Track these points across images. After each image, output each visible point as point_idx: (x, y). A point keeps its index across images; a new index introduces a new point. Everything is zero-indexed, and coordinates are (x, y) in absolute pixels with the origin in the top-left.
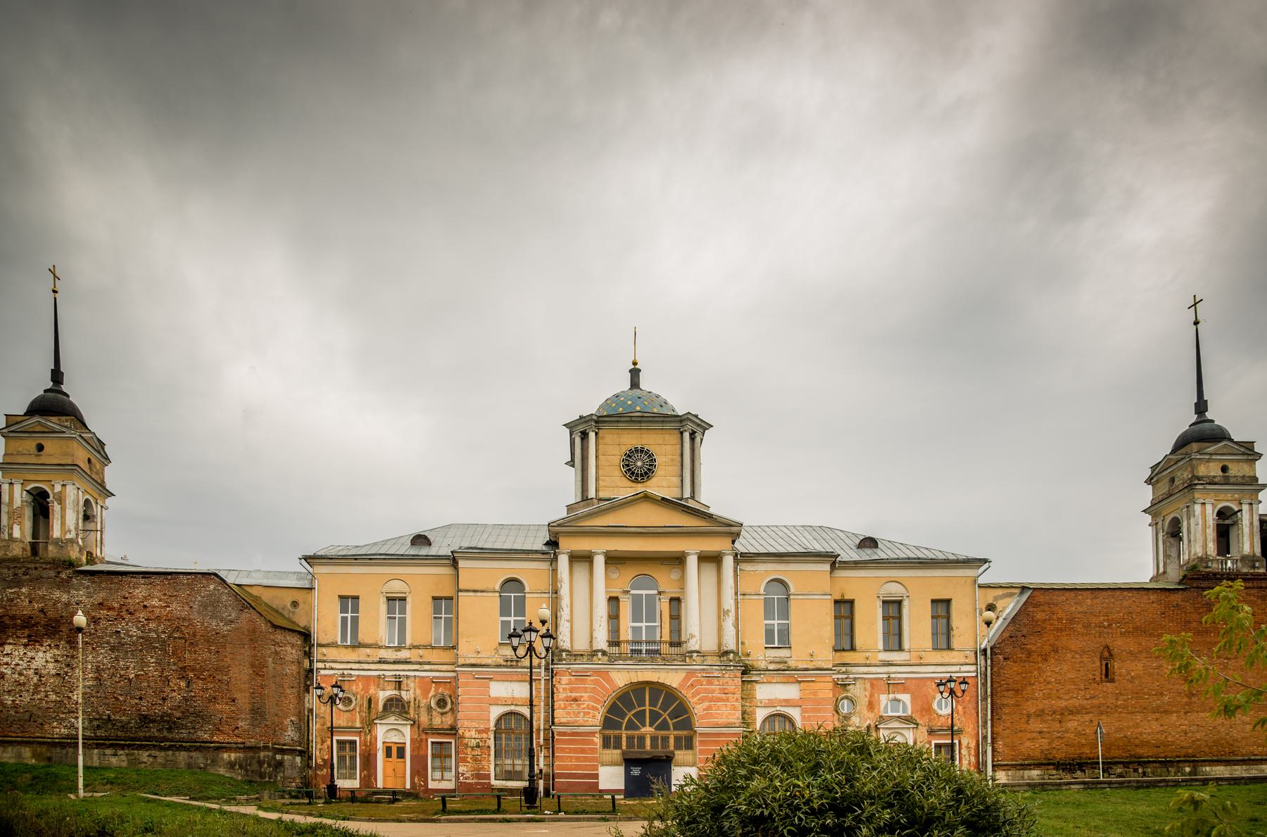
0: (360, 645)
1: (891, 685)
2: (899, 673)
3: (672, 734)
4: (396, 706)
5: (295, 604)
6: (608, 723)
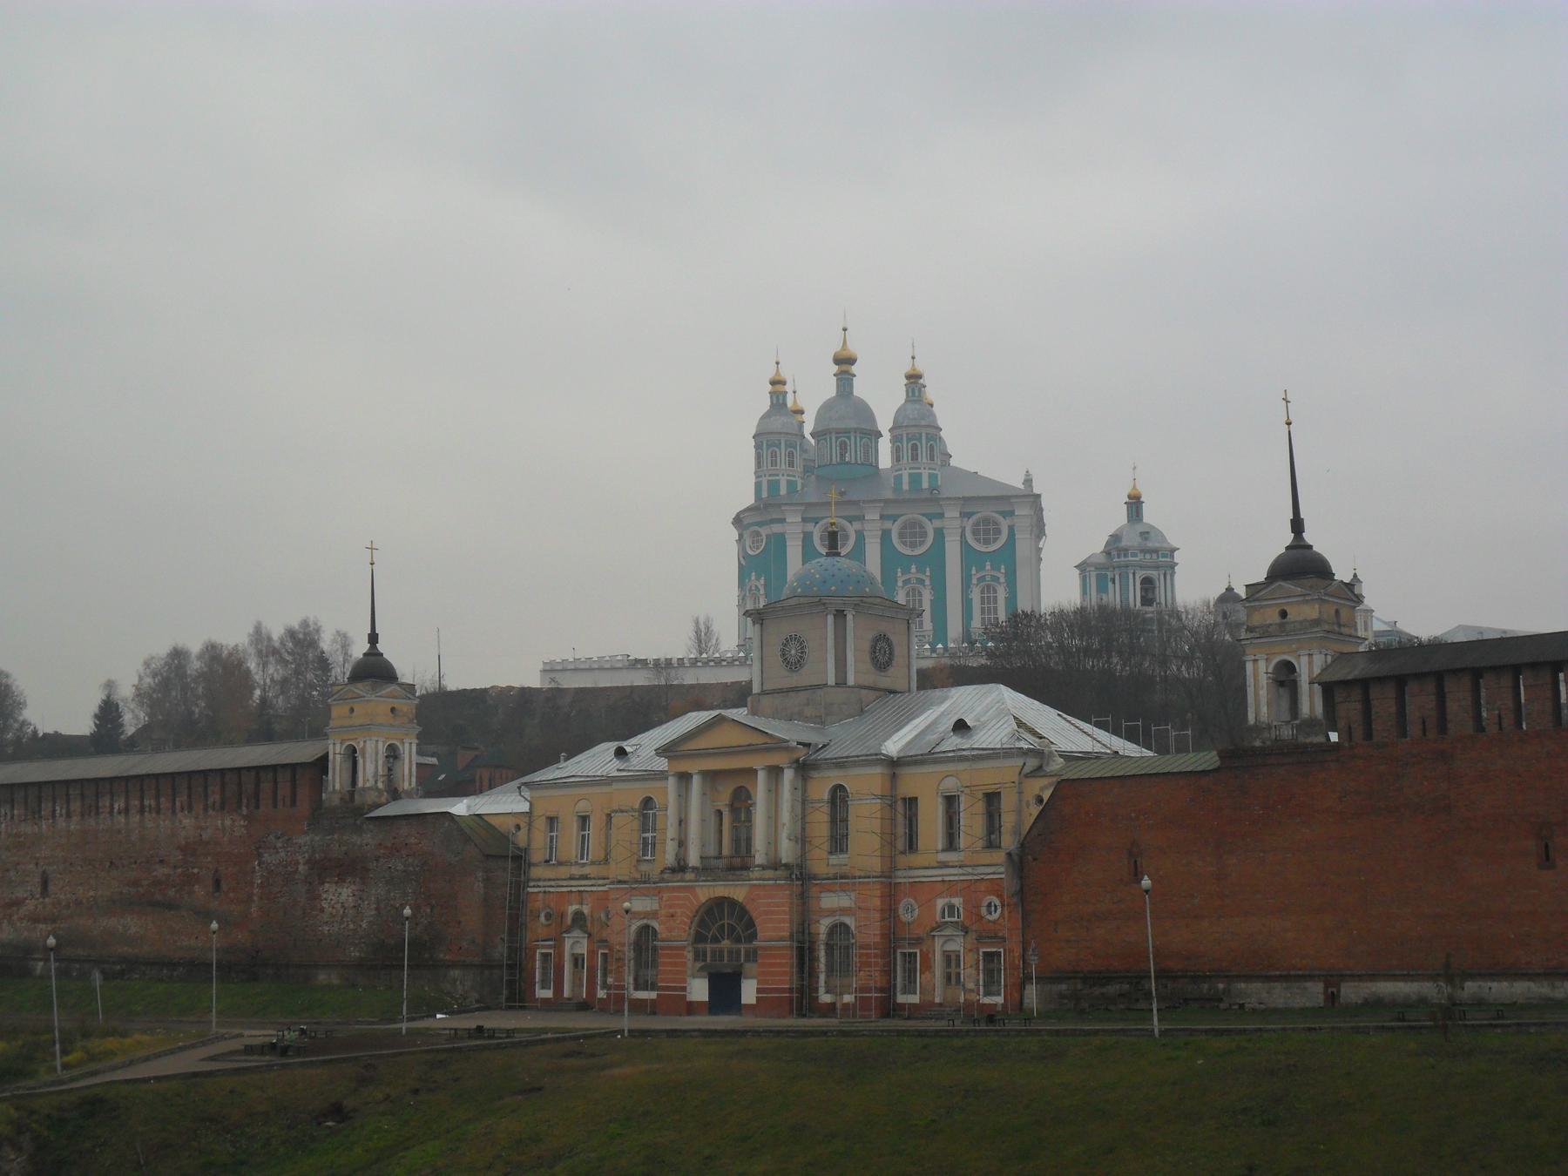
0: (560, 863)
2: (951, 874)
3: (743, 947)
5: (518, 827)
6: (699, 938)
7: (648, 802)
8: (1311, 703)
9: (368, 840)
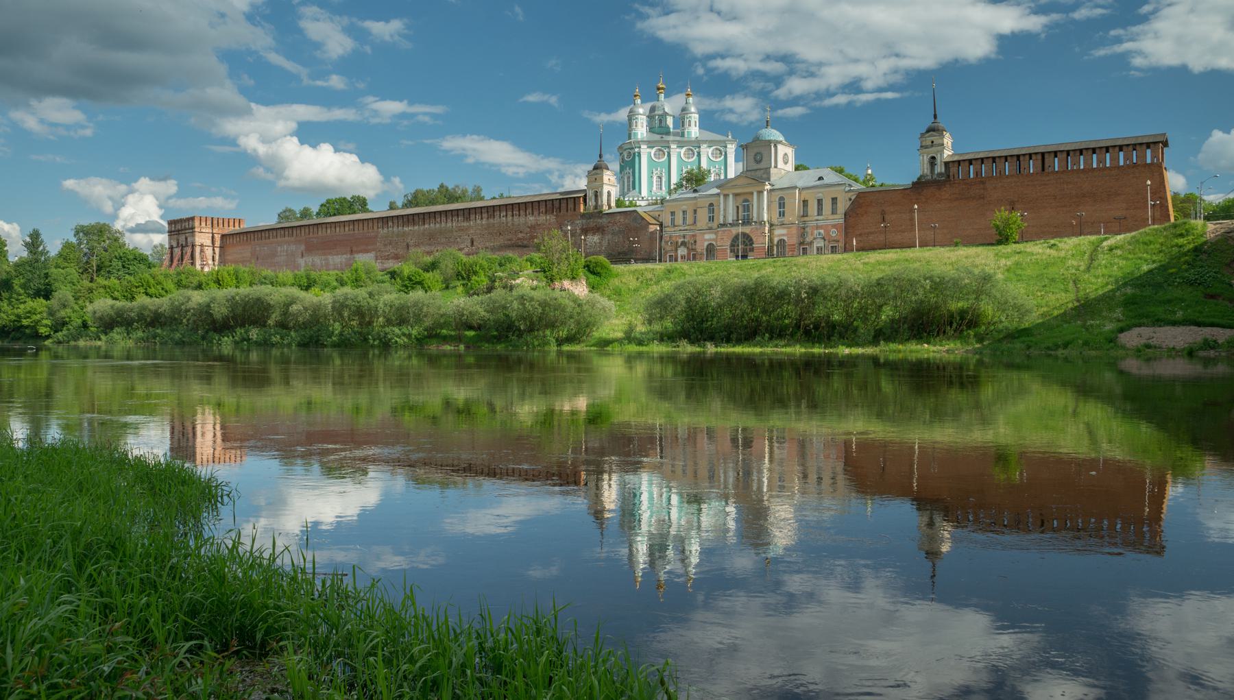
1: (818, 227)
2: (820, 223)
4: (684, 244)
7: (711, 205)
8: (940, 169)
9: (604, 221)
